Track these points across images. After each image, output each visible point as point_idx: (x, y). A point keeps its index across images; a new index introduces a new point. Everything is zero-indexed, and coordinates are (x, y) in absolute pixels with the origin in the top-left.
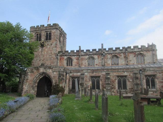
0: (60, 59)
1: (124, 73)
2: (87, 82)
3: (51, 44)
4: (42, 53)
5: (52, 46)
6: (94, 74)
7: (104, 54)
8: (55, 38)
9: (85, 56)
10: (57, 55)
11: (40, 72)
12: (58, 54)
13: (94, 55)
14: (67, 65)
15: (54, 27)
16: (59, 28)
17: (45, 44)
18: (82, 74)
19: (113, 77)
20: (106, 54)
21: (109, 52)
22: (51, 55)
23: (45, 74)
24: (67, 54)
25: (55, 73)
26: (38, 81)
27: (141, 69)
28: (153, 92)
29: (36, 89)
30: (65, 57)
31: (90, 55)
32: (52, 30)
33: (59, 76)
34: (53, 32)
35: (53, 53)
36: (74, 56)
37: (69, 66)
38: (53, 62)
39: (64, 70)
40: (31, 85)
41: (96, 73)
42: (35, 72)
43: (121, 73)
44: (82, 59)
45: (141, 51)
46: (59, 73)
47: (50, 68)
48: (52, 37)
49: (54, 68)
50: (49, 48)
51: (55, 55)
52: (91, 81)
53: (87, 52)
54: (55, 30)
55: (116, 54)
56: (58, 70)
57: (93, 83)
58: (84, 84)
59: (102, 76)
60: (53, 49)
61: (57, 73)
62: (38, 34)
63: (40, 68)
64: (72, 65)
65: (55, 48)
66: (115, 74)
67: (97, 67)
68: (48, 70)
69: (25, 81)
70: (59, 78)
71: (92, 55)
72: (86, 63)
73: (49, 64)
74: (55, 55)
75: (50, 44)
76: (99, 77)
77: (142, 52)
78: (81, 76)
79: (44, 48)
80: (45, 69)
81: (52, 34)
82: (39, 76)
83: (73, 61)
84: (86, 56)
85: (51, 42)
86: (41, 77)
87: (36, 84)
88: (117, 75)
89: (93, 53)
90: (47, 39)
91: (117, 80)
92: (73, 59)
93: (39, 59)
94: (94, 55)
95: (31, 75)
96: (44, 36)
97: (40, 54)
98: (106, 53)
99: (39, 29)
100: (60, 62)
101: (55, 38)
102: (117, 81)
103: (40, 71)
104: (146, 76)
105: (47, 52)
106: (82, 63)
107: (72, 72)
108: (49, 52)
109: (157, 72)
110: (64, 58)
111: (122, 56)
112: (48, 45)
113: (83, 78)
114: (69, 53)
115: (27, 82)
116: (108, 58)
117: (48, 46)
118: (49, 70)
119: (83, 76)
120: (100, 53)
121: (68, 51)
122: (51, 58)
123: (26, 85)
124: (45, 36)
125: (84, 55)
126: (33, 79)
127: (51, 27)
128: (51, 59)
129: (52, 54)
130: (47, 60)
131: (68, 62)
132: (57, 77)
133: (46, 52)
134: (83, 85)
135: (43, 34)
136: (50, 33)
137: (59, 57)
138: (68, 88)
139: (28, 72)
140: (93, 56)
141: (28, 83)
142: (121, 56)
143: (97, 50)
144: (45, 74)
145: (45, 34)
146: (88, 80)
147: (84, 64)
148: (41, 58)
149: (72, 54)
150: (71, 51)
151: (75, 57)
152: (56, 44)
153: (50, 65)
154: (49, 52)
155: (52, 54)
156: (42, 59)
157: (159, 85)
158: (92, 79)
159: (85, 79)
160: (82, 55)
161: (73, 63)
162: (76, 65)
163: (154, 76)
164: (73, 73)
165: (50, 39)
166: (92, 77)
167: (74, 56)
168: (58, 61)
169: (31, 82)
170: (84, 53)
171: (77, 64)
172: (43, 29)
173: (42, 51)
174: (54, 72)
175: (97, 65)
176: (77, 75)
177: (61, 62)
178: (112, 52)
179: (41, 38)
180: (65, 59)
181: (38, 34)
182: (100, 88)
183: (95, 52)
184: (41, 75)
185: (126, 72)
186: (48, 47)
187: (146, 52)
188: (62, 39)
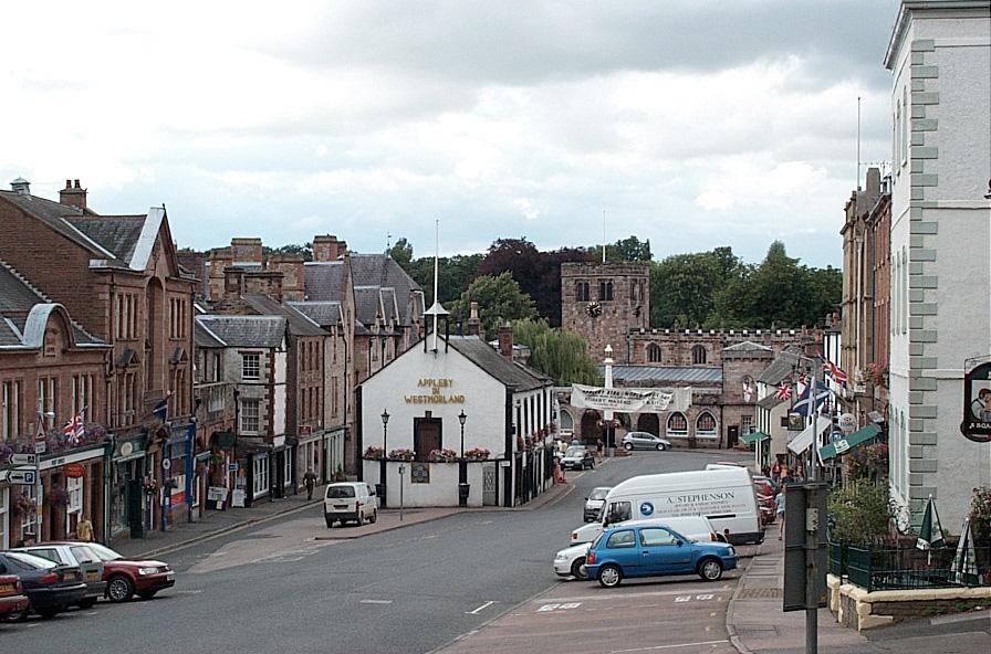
0: (635, 347)
3: (614, 312)
30: (647, 344)
48: (615, 294)
62: (580, 284)
64: (660, 360)
81: (615, 288)
105: (605, 328)
135: (594, 285)
136: (610, 284)
140: (702, 344)
165: (610, 298)
188: (637, 290)
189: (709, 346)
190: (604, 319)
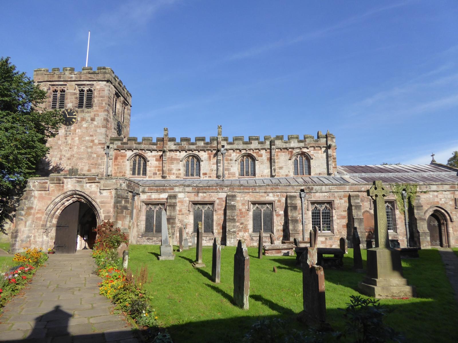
0: (116, 158)
1: (268, 195)
2: (183, 214)
3: (93, 120)
4: (66, 139)
5: (95, 123)
6: (201, 197)
7: (222, 149)
8: (104, 104)
9: (178, 153)
10: (108, 147)
11: (65, 191)
12: (111, 146)
13: (199, 152)
14: (134, 173)
15: (100, 77)
16: (113, 81)
17: (75, 118)
18: (170, 197)
19: (243, 204)
20: (227, 150)
21: (235, 146)
22: (91, 147)
23: (78, 196)
24: (135, 146)
25: (105, 193)
26: (59, 211)
27: (302, 188)
28: (326, 239)
29: (53, 233)
31: (191, 150)
32: (94, 83)
33: (117, 202)
34: (98, 87)
35: (96, 141)
36: (151, 151)
37: (139, 174)
38: (96, 164)
39: (128, 186)
40: (41, 223)
41: (205, 195)
42: (51, 189)
43: (262, 196)
44: (172, 160)
45: (303, 148)
46: (116, 194)
47: (92, 180)
48: (96, 101)
49: (102, 182)
50: (86, 128)
51: (103, 146)
52: (192, 213)
53: (183, 143)
54: (105, 83)
55: (250, 152)
56: (115, 187)
57: (197, 218)
58: (177, 221)
59: (217, 201)
60: (96, 131)
61: (111, 192)
62: (56, 91)
63: (65, 180)
64: (145, 173)
65: (103, 130)
66: (249, 198)
67: (205, 179)
68: (88, 185)
69: (23, 212)
70: (115, 206)
71: (195, 150)
72: (179, 170)
73: (86, 168)
74: (103, 146)
75: (89, 119)
76: (212, 204)
77: (305, 150)
78: (169, 201)
79: (72, 127)
80: (79, 182)
81: (96, 93)
82: (62, 200)
83: (148, 164)
84: (180, 152)
85: (92, 114)
86: (67, 204)
87: (55, 221)
88: (253, 199)
89: (196, 147)
90: (80, 105)
91: (252, 210)
92: (149, 159)
93: (59, 156)
94: (199, 152)
95: (41, 198)
96: (73, 97)
97: (60, 142)
98: (227, 147)
99: (60, 77)
100: (115, 165)
101: (102, 104)
102: (251, 213)
103: (65, 187)
104: (313, 203)
106: (170, 170)
107: (147, 189)
108: (87, 138)
109: (336, 194)
110: (125, 156)
111: (263, 156)
112: (83, 119)
113: (173, 206)
114: (139, 143)
115: (28, 214)
116: (231, 160)
117: (84, 122)
118: (90, 186)
119: (173, 201)
120: (214, 147)
121: (135, 139)
122: (92, 153)
123: (26, 223)
124: (76, 98)
125: (176, 150)
126: (45, 208)
127: (92, 76)
128: (90, 157)
129: (95, 145)
130: (81, 159)
131: (134, 164)
132: (112, 204)
133: (77, 138)
134: (174, 223)
137: (112, 153)
138: (135, 229)
139: (32, 188)
140: (196, 153)
141: (31, 217)
142: (261, 156)
143: (208, 140)
144: (78, 196)
145: (78, 92)
146: (185, 210)
147: (174, 171)
148: (64, 153)
149: (147, 147)
150: (144, 139)
151: (154, 153)
152: (107, 120)
153: (89, 170)
154: (87, 138)
155: (95, 145)
156: (68, 155)
157: (338, 223)
158: (194, 209)
159: (178, 208)
160: (171, 151)
161: (148, 169)
162: (155, 174)
163: (330, 203)
164: (150, 194)
165: (89, 105)
166: (195, 203)
167: (151, 152)
168: (111, 162)
169: (39, 215)
170: (175, 144)
171: (159, 170)
172: (71, 78)
173: (66, 136)
174: (101, 191)
175: (205, 174)
176: (159, 199)
177: (118, 165)
178: (241, 146)
179: (66, 101)
180: (127, 158)
181: (56, 91)
182: (212, 229)
183: (202, 144)
184: (69, 198)
185: (271, 194)
186: (85, 125)
187: (315, 150)
189: (203, 155)
190: (80, 127)
